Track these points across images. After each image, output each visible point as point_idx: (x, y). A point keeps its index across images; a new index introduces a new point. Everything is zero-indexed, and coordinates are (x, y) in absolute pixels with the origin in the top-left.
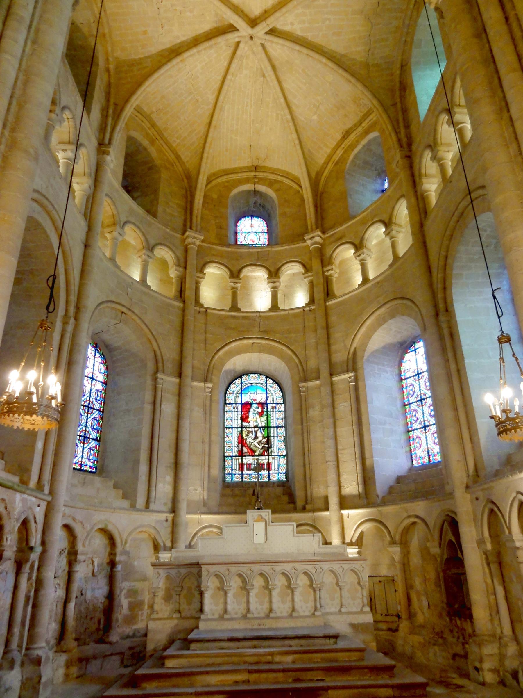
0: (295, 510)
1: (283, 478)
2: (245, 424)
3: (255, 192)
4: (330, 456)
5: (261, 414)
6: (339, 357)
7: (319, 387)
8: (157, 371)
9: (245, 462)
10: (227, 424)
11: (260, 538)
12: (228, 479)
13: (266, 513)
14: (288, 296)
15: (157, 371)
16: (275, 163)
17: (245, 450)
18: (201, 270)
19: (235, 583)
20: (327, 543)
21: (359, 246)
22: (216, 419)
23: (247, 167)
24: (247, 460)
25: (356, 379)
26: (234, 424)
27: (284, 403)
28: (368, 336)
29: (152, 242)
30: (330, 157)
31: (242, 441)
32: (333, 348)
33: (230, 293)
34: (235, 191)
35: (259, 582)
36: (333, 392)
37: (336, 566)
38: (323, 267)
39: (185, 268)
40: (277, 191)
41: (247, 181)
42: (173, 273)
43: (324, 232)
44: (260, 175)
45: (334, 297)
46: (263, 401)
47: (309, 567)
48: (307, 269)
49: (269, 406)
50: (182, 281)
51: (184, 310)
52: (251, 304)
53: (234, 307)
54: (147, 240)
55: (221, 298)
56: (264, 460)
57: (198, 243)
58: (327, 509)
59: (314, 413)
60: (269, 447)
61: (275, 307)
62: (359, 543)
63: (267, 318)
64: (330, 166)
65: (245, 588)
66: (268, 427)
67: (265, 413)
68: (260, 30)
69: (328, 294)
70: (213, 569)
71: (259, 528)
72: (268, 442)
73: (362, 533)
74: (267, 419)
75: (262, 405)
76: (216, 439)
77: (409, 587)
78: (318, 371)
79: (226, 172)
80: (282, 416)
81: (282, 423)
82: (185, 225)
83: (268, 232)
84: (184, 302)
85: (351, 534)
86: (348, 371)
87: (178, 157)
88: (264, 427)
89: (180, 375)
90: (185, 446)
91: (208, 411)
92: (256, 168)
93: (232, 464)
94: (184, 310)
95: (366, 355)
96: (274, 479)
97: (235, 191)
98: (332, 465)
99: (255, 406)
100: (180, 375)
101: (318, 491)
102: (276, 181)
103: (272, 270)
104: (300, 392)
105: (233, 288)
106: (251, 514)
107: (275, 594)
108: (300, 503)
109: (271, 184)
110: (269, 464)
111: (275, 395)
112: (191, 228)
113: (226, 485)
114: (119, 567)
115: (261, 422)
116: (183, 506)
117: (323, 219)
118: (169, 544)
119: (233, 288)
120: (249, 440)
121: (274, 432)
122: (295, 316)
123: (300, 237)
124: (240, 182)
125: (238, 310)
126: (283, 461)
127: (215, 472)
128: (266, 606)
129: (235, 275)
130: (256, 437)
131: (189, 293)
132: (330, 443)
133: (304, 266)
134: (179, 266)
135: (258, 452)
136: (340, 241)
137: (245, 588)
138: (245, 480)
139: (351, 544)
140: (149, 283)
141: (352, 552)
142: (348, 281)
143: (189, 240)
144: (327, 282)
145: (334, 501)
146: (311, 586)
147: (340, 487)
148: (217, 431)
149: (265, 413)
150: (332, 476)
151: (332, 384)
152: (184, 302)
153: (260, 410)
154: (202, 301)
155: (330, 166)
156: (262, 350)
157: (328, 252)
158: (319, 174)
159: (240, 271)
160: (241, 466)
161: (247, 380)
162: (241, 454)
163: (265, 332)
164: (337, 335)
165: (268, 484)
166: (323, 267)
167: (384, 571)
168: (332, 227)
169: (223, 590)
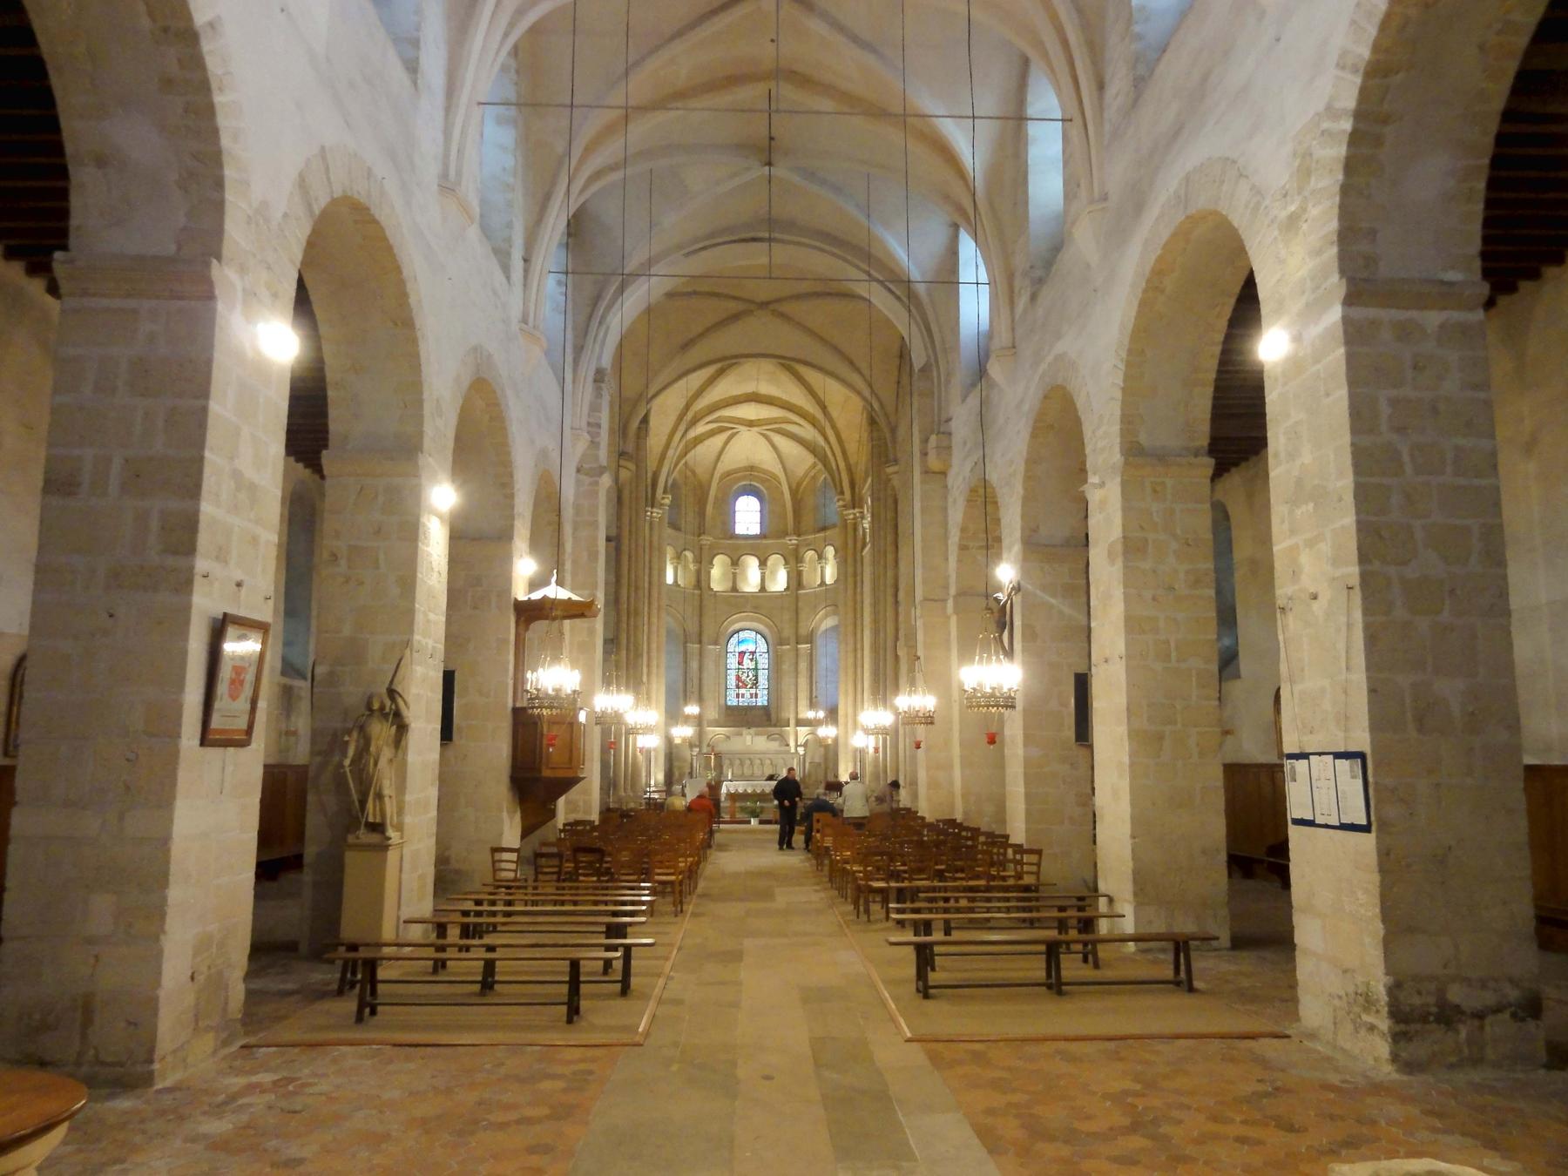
0: (770, 726)
2: (740, 667)
3: (750, 485)
4: (793, 697)
5: (752, 660)
6: (803, 631)
7: (789, 650)
8: (686, 642)
9: (740, 692)
10: (728, 667)
11: (749, 743)
12: (729, 703)
13: (753, 730)
14: (774, 573)
15: (686, 642)
16: (765, 466)
17: (740, 684)
18: (711, 563)
19: (738, 762)
20: (788, 745)
21: (821, 556)
22: (722, 669)
23: (745, 467)
24: (742, 691)
25: (811, 649)
26: (733, 667)
27: (768, 652)
28: (821, 621)
29: (679, 551)
30: (806, 475)
31: (738, 678)
32: (801, 624)
33: (731, 576)
34: (736, 487)
35: (748, 762)
36: (797, 655)
37: (784, 756)
38: (797, 563)
39: (701, 563)
40: (767, 489)
41: (744, 478)
42: (692, 567)
43: (799, 535)
44: (756, 473)
45: (803, 588)
46: (753, 650)
47: (770, 756)
48: (787, 563)
49: (758, 654)
50: (698, 572)
51: (701, 595)
52: (745, 579)
53: (734, 589)
54: (677, 553)
55: (724, 574)
56: (753, 691)
57: (709, 543)
58: (789, 726)
59: (785, 667)
60: (757, 683)
61: (763, 588)
62: (805, 745)
63: (758, 597)
64: (807, 480)
65: (742, 764)
66: (756, 669)
68: (755, 429)
69: (800, 585)
70: (728, 756)
71: (749, 738)
72: (756, 679)
73: (807, 741)
74: (756, 664)
75: (753, 653)
76: (722, 681)
77: (826, 769)
78: (789, 639)
79: (728, 474)
80: (767, 661)
81: (767, 667)
82: (699, 528)
84: (701, 589)
85: (801, 740)
86: (807, 643)
87: (694, 473)
88: (753, 669)
89: (700, 642)
90: (705, 689)
91: (717, 666)
92: (752, 468)
93: (732, 694)
94: (701, 595)
95: (819, 633)
96: (759, 704)
97: (736, 487)
98: (793, 701)
99: (747, 654)
100: (700, 642)
101: (785, 715)
102: (768, 480)
103: (762, 560)
104: (777, 652)
105: (733, 573)
106: (745, 731)
107: (755, 767)
108: (773, 722)
109: (763, 481)
110: (756, 694)
111: (763, 646)
113: (729, 708)
115: (752, 665)
116: (705, 723)
117: (799, 523)
118: (697, 743)
119: (733, 573)
120: (743, 678)
121: (760, 672)
122: (776, 597)
123: (785, 534)
124: (739, 479)
125: (737, 591)
126: (766, 692)
127: (722, 702)
128: (751, 772)
129: (735, 563)
130: (748, 676)
131: (704, 584)
132: (793, 687)
133: (785, 559)
134: (697, 562)
136: (809, 546)
137: (742, 764)
138: (740, 704)
139: (801, 746)
140: (679, 583)
141: (801, 751)
142: (815, 570)
143: (704, 542)
144: (800, 574)
145: (792, 722)
146: (771, 764)
147: (797, 713)
148: (723, 676)
150: (792, 708)
151: (797, 650)
152: (701, 589)
153: (751, 657)
154: (712, 586)
155: (807, 480)
156: (752, 620)
157: (802, 550)
158: (799, 485)
159: (739, 559)
160: (738, 696)
161: (742, 635)
162: (738, 687)
163: (756, 608)
164: (802, 616)
165: (756, 707)
166: (797, 563)
167: (817, 760)
168: (806, 533)
169: (732, 765)
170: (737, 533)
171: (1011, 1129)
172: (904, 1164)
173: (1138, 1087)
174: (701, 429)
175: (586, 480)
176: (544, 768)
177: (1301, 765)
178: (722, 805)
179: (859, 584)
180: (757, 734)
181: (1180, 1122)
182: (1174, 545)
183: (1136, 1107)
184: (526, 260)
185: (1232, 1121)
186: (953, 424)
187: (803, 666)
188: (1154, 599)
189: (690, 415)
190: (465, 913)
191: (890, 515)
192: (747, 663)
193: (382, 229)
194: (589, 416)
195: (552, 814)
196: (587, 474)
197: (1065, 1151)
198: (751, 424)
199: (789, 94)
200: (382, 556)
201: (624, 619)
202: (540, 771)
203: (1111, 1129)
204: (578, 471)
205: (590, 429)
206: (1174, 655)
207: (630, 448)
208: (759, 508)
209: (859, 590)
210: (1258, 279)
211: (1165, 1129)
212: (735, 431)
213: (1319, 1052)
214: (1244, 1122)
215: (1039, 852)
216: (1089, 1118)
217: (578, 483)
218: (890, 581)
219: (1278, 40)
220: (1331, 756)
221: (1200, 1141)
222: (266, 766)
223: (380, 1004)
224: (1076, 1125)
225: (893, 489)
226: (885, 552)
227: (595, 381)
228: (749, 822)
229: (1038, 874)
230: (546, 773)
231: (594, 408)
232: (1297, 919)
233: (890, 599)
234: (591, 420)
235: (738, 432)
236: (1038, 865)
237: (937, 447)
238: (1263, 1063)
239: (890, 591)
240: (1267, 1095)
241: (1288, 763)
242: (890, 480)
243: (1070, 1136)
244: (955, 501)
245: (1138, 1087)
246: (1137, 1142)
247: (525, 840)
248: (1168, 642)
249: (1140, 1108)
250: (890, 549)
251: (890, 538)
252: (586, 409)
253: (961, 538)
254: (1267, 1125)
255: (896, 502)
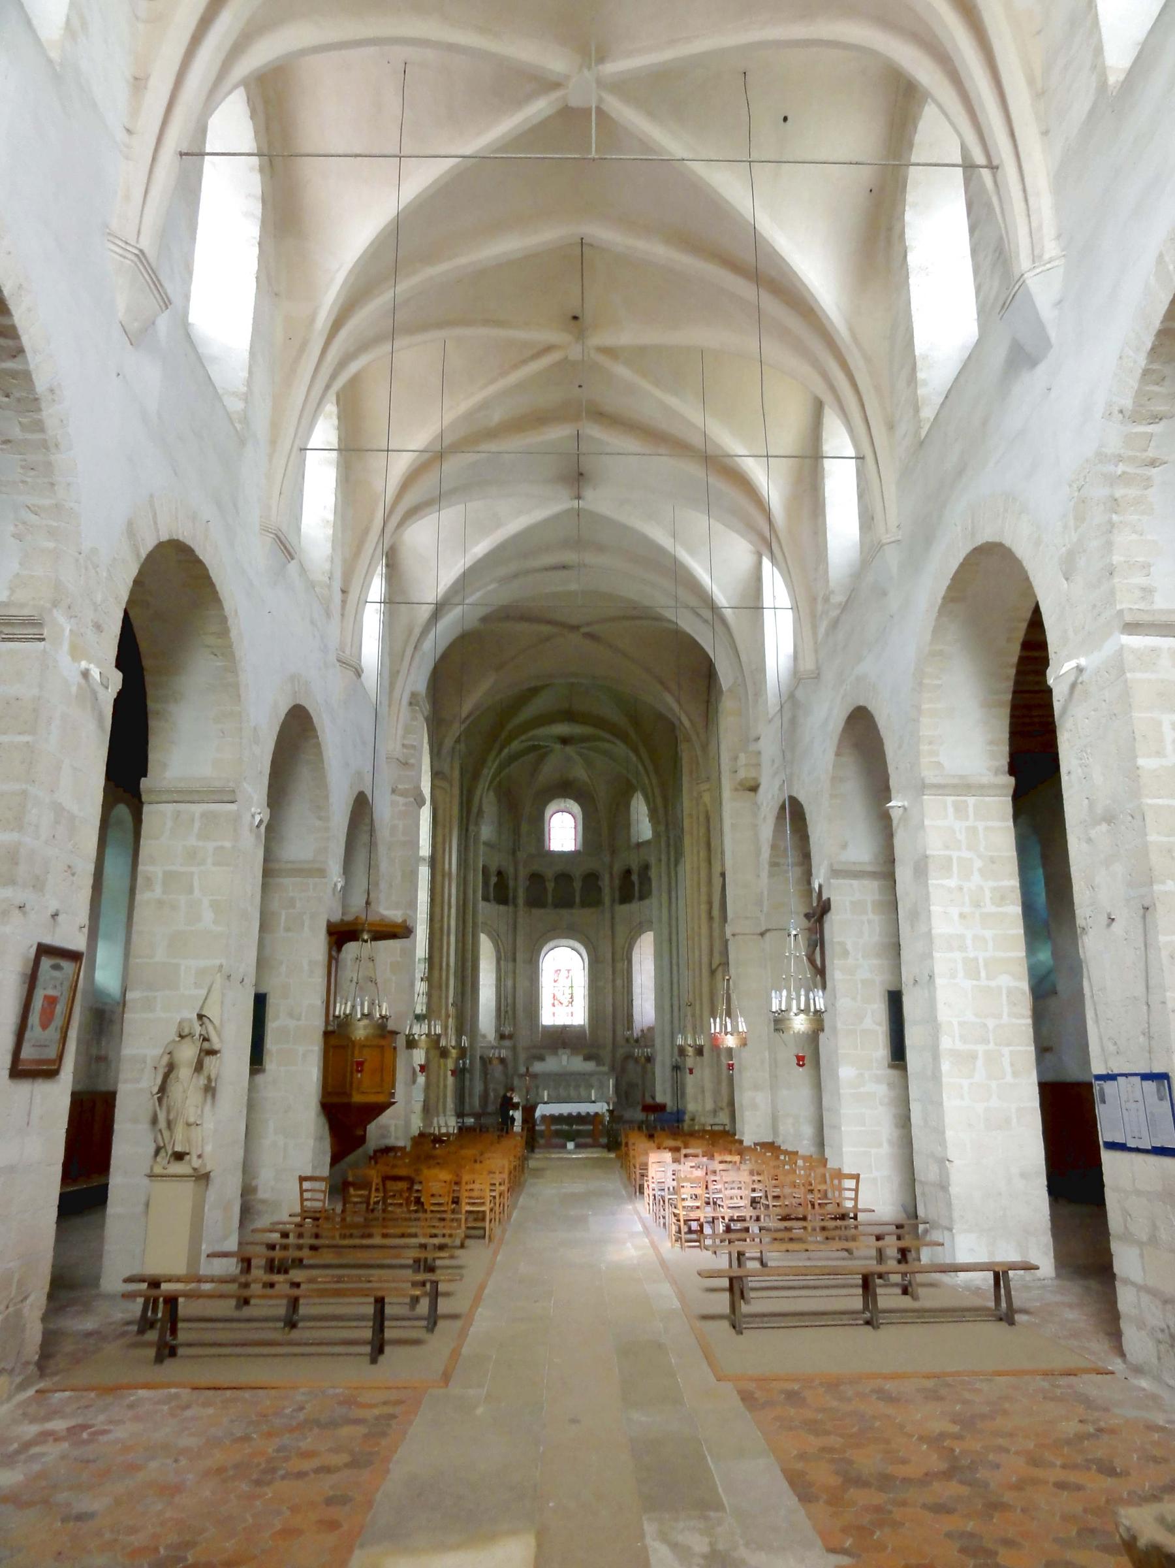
1: (582, 1023)
2: (555, 984)
11: (564, 1062)
13: (568, 1051)
17: (556, 1002)
24: (558, 1008)
56: (570, 1009)
67: (570, 978)
68: (570, 750)
71: (565, 1058)
83: (575, 828)
89: (514, 960)
106: (560, 1051)
112: (519, 850)
114: (489, 1076)
120: (559, 996)
135: (565, 1003)
149: (570, 978)
162: (554, 1005)
170: (551, 849)
171: (823, 1475)
172: (712, 1514)
173: (956, 1429)
174: (516, 745)
175: (401, 800)
176: (354, 1093)
177: (1109, 1087)
178: (537, 1128)
179: (674, 900)
180: (572, 1054)
181: (998, 1466)
182: (978, 864)
183: (952, 1450)
184: (343, 592)
185: (1053, 1465)
186: (762, 742)
187: (619, 982)
188: (962, 916)
189: (504, 735)
190: (272, 1247)
191: (703, 830)
192: (563, 981)
193: (206, 570)
194: (404, 737)
195: (362, 1140)
196: (402, 795)
197: (877, 1498)
198: (565, 741)
199: (594, 431)
200: (196, 884)
201: (437, 936)
202: (350, 1095)
203: (926, 1474)
204: (394, 791)
205: (405, 751)
206: (983, 974)
207: (446, 768)
208: (573, 825)
209: (674, 905)
210: (1043, 609)
211: (982, 1474)
212: (548, 749)
213: (1144, 1390)
214: (1064, 1467)
215: (857, 1177)
216: (904, 1462)
217: (393, 804)
218: (704, 898)
219: (1049, 389)
220: (1139, 1078)
221: (1019, 1487)
222: (73, 1094)
223: (182, 1345)
224: (890, 1469)
225: (705, 805)
226: (698, 868)
227: (411, 704)
228: (565, 1146)
229: (856, 1199)
230: (357, 1098)
231: (408, 730)
232: (1115, 1247)
233: (704, 916)
234: (406, 742)
235: (551, 751)
236: (856, 1190)
237: (746, 765)
238: (1087, 1402)
239: (704, 907)
240: (1089, 1436)
241: (1097, 1086)
242: (701, 797)
243: (885, 1482)
244: (765, 818)
245: (956, 1429)
246: (952, 1489)
247: (337, 1167)
248: (976, 959)
249: (958, 1450)
250: (703, 865)
251: (703, 854)
252: (400, 732)
253: (771, 856)
254: (1089, 1469)
255: (708, 819)
